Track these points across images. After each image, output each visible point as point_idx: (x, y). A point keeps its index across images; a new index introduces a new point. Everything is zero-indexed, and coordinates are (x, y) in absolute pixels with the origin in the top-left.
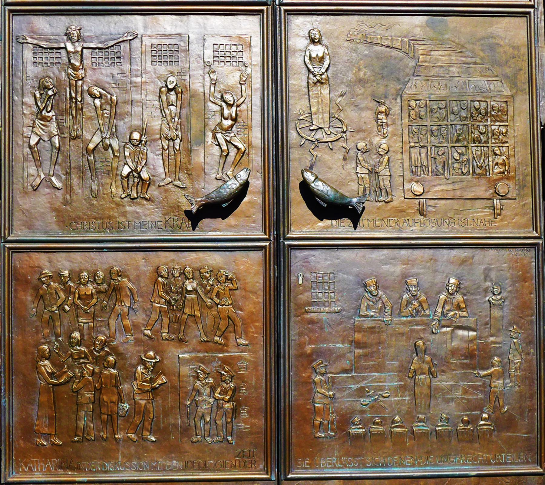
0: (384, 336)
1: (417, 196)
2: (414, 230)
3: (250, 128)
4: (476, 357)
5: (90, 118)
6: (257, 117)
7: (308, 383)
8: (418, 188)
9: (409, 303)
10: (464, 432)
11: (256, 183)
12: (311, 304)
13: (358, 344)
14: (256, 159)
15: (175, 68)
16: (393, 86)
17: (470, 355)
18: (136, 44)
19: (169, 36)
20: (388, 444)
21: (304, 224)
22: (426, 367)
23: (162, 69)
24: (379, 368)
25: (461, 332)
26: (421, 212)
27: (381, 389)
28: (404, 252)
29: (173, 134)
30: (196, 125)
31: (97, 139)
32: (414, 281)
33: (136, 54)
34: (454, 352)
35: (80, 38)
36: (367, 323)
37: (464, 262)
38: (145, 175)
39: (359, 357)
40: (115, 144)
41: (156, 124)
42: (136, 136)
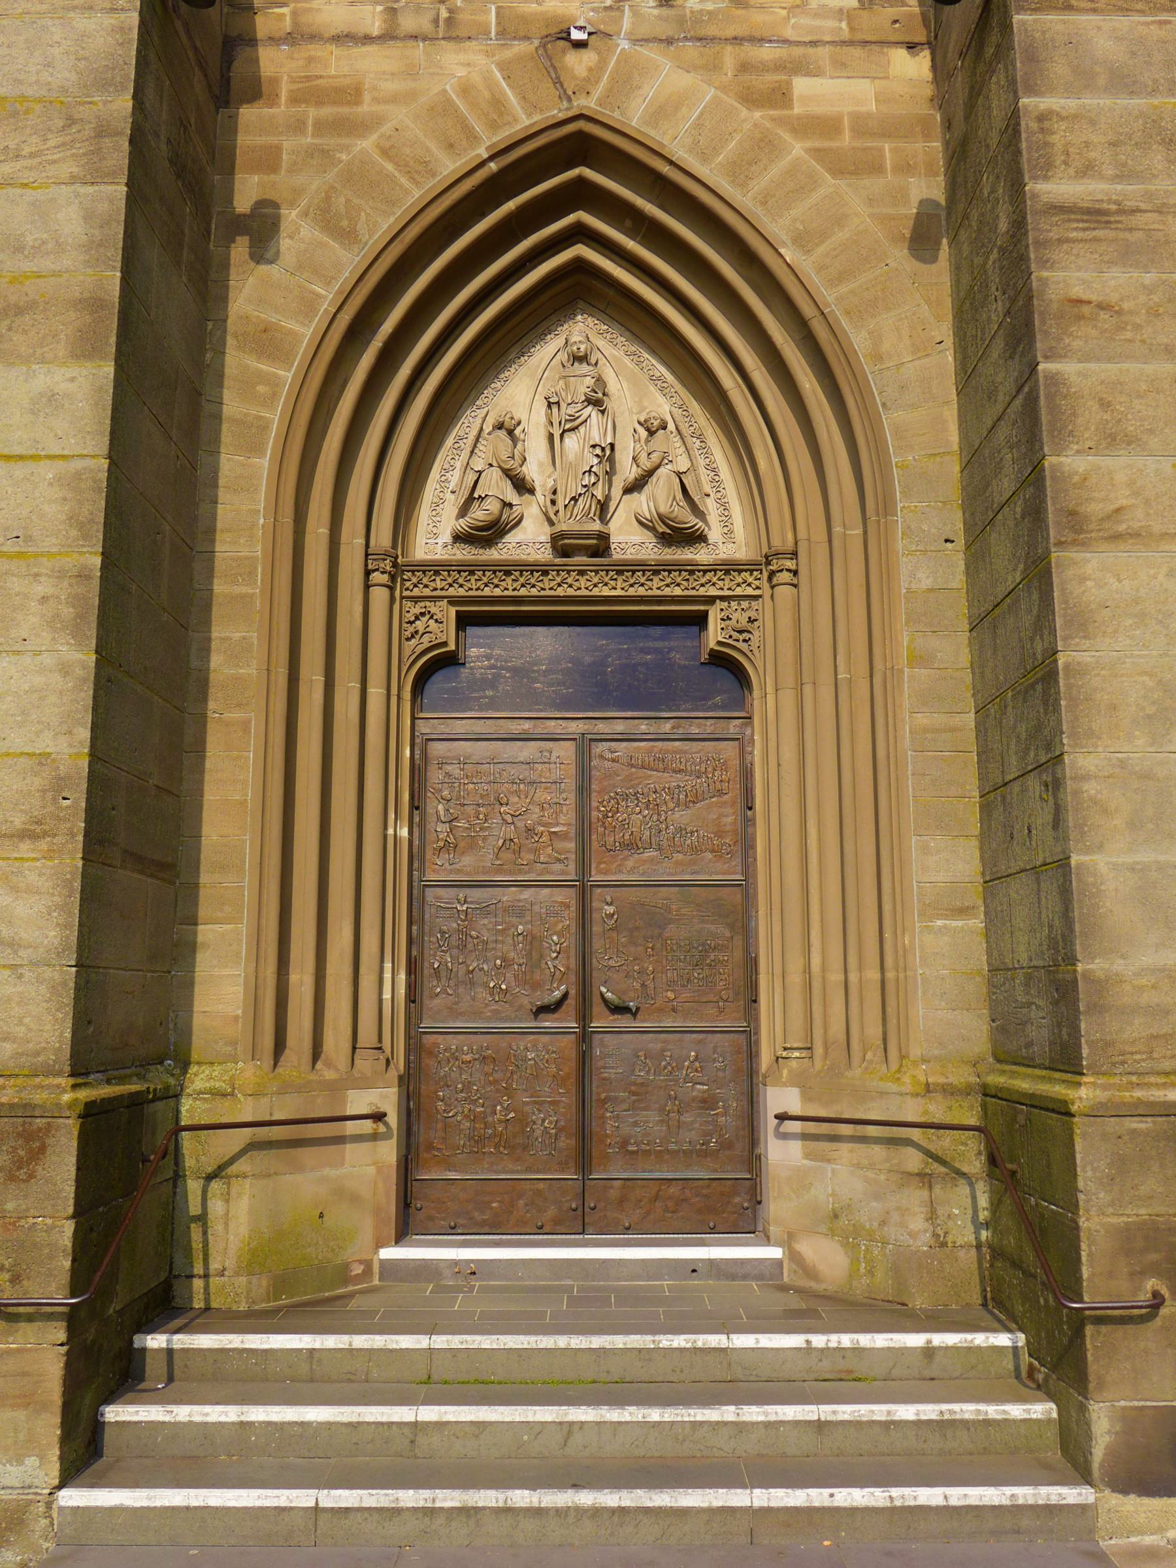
0: (650, 1089)
1: (671, 1001)
2: (668, 1023)
3: (568, 958)
4: (707, 1103)
5: (471, 951)
6: (573, 952)
7: (603, 1117)
8: (671, 995)
9: (665, 1068)
10: (700, 1151)
11: (573, 992)
12: (605, 1068)
13: (634, 1094)
14: (573, 978)
15: (524, 920)
16: (656, 932)
17: (704, 1101)
18: (500, 905)
19: (519, 901)
20: (653, 1157)
21: (601, 1021)
22: (676, 1108)
23: (514, 920)
24: (647, 1109)
25: (698, 1086)
26: (674, 1010)
27: (647, 1122)
28: (662, 1035)
29: (521, 961)
30: (535, 956)
31: (475, 964)
32: (669, 1054)
33: (500, 912)
34: (694, 1099)
35: (465, 902)
36: (639, 1081)
37: (700, 1042)
38: (503, 987)
39: (634, 1102)
40: (486, 967)
41: (512, 955)
42: (498, 962)
